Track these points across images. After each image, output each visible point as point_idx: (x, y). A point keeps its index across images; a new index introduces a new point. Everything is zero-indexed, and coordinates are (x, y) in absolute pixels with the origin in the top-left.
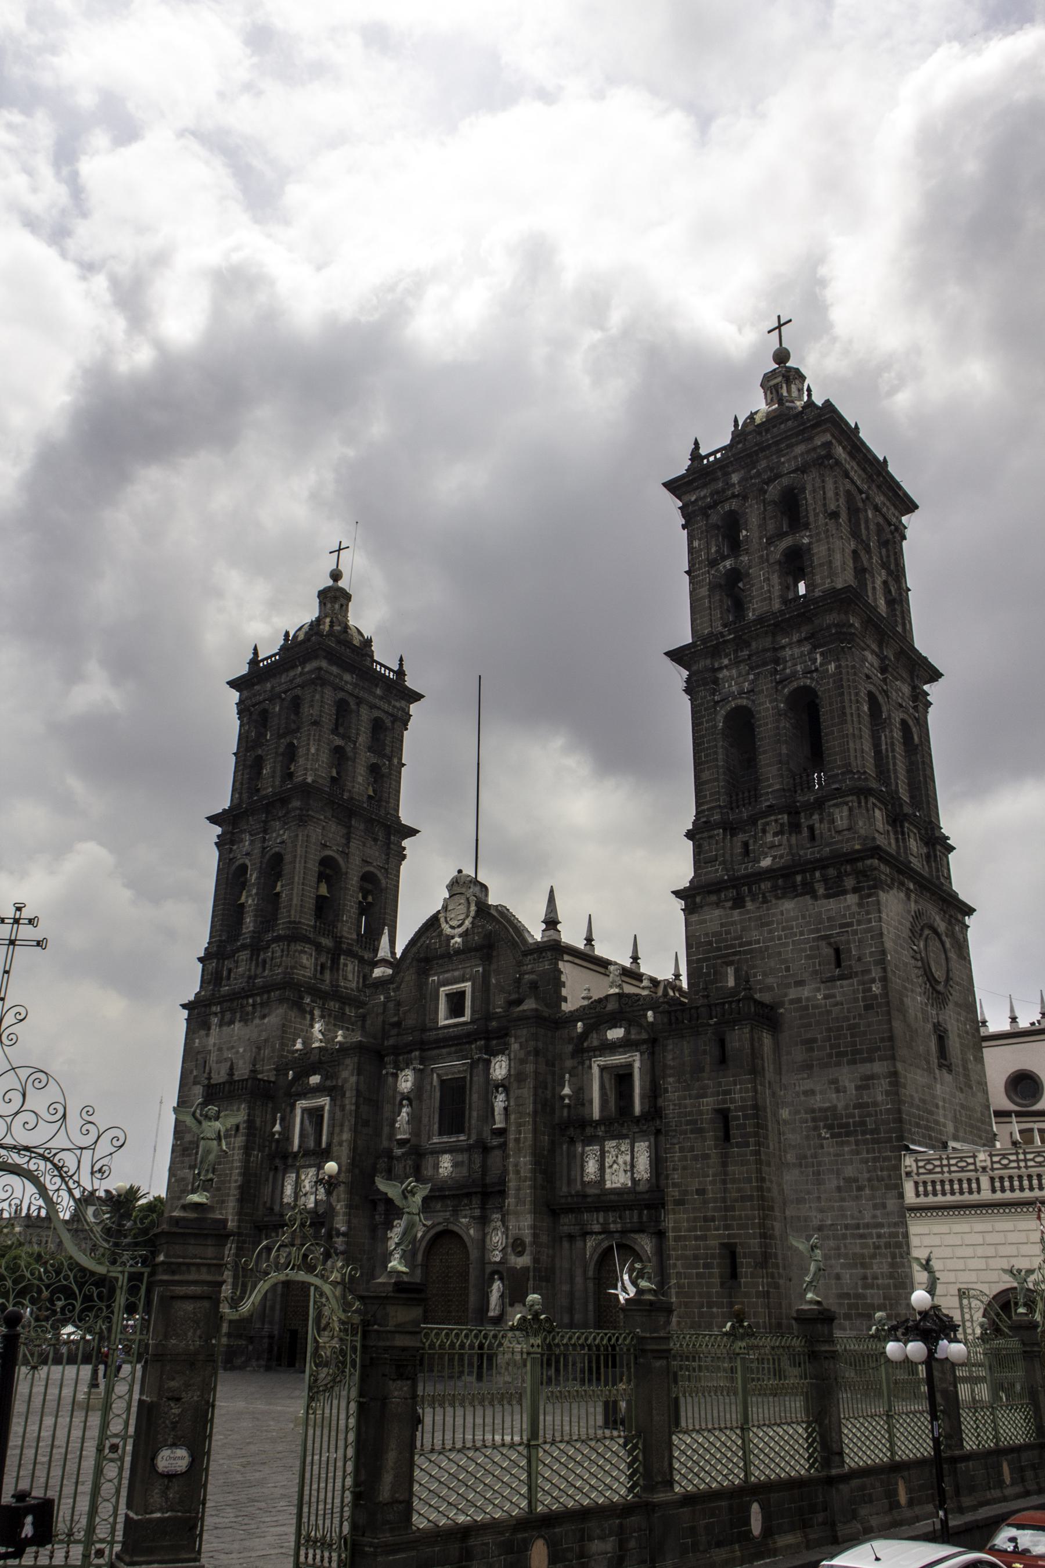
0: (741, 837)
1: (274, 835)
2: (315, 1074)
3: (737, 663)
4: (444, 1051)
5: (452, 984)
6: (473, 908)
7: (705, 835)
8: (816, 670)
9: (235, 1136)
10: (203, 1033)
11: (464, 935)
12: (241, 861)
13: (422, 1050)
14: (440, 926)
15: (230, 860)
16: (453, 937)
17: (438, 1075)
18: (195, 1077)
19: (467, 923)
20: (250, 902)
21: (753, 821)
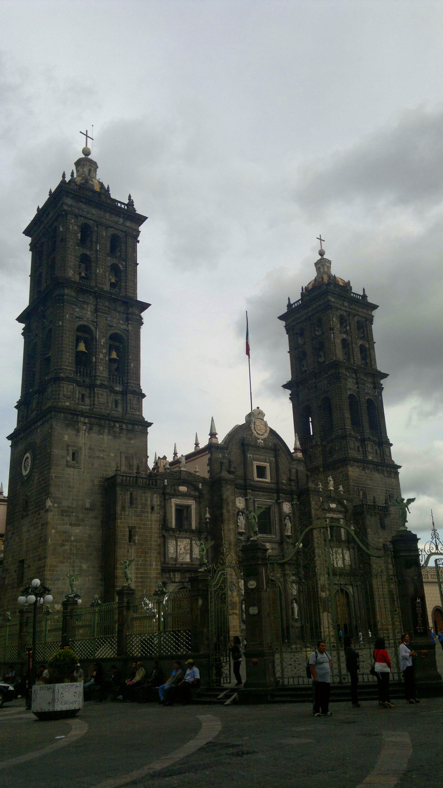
0: (357, 444)
1: (115, 320)
2: (183, 486)
3: (353, 378)
4: (261, 493)
5: (259, 461)
6: (269, 429)
7: (350, 438)
8: (376, 396)
9: (151, 513)
10: (71, 432)
11: (264, 440)
12: (85, 323)
13: (251, 490)
14: (250, 430)
15: (76, 317)
16: (258, 439)
17: (258, 504)
18: (67, 461)
19: (266, 435)
20: (101, 356)
21: (363, 441)
